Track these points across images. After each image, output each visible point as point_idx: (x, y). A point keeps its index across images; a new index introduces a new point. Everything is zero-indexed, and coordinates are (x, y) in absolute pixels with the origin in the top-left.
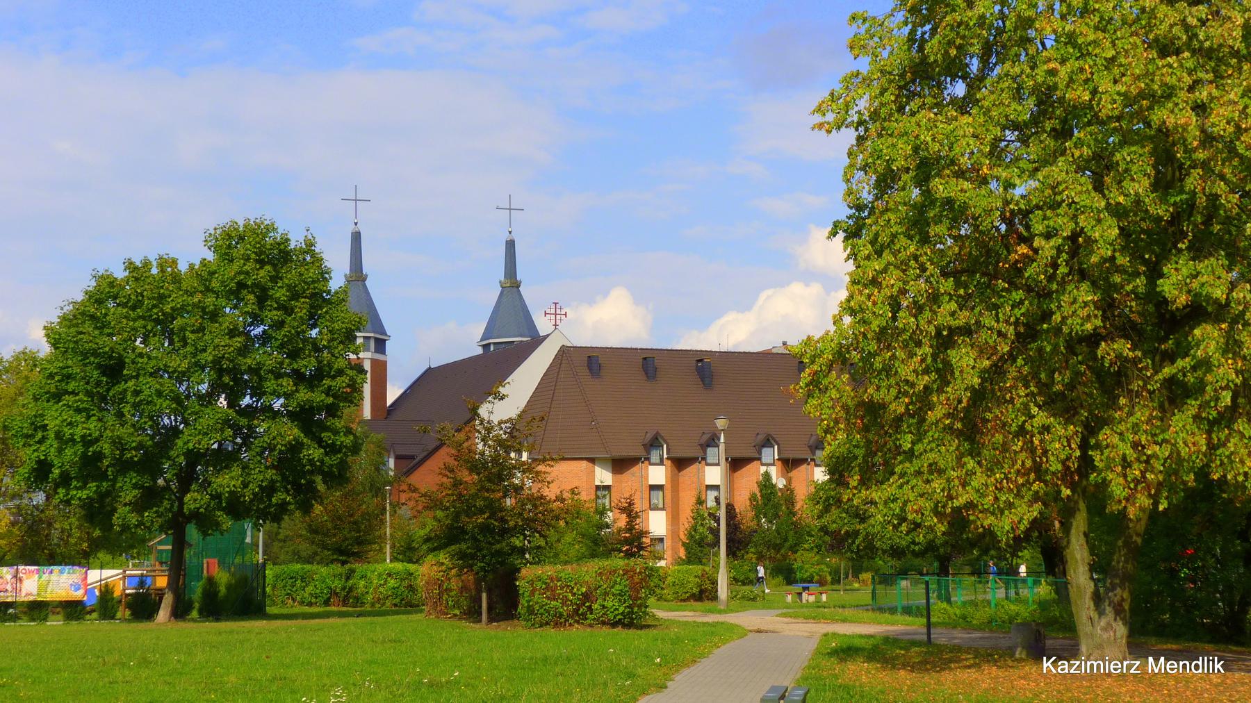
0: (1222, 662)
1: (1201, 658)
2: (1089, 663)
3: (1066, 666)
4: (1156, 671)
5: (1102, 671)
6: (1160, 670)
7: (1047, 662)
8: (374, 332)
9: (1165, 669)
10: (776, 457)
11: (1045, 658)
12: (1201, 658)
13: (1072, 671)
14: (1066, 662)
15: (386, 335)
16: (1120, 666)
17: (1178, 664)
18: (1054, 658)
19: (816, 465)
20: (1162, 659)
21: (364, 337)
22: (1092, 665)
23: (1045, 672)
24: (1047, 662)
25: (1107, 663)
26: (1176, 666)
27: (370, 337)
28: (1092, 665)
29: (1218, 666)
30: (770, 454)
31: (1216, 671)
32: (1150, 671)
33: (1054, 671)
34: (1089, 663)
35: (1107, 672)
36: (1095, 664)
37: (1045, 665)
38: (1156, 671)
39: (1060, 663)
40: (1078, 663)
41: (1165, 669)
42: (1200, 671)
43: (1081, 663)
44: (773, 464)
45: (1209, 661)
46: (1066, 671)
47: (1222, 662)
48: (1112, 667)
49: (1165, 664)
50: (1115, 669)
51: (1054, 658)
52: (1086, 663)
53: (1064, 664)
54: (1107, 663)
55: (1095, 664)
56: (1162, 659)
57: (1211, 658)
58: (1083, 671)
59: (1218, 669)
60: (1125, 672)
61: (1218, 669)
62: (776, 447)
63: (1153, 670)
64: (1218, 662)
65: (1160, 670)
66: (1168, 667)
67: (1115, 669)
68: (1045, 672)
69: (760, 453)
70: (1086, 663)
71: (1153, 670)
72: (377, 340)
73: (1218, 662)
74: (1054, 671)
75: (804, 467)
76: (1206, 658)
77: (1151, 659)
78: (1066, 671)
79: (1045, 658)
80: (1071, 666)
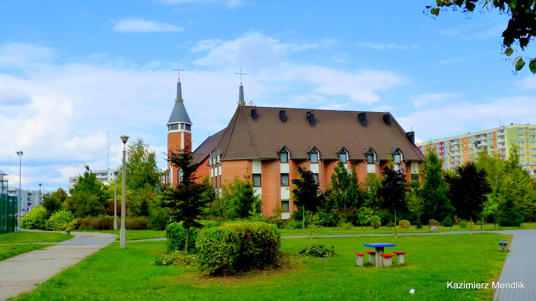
3: (457, 286)
8: (185, 121)
10: (348, 159)
11: (448, 282)
15: (191, 123)
18: (452, 282)
19: (368, 163)
21: (181, 124)
23: (448, 288)
27: (183, 124)
30: (344, 158)
33: (452, 288)
37: (448, 285)
39: (454, 284)
44: (346, 163)
46: (457, 288)
51: (452, 282)
62: (347, 154)
68: (448, 288)
69: (339, 157)
72: (187, 125)
74: (452, 288)
75: (362, 165)
78: (457, 288)
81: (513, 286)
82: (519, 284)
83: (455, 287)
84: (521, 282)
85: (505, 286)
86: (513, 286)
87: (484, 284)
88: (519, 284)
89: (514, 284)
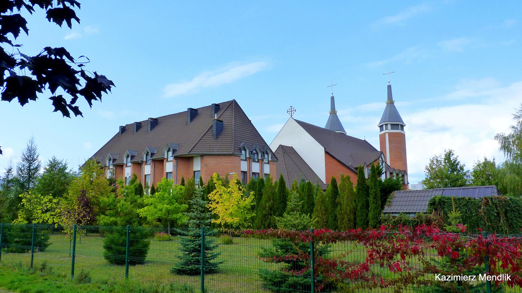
0: (510, 276)
1: (501, 274)
2: (454, 276)
3: (445, 278)
4: (483, 280)
5: (460, 280)
6: (484, 279)
7: (437, 276)
9: (486, 279)
12: (501, 274)
13: (447, 280)
14: (445, 276)
16: (467, 278)
17: (492, 277)
18: (440, 274)
20: (485, 275)
22: (456, 277)
24: (437, 276)
25: (462, 276)
26: (491, 278)
28: (456, 278)
29: (508, 278)
31: (507, 280)
32: (480, 280)
34: (454, 276)
35: (462, 280)
36: (457, 277)
37: (436, 277)
38: (483, 280)
39: (442, 277)
40: (450, 276)
41: (486, 279)
42: (501, 280)
43: (451, 277)
45: (504, 275)
46: (445, 280)
47: (510, 276)
48: (464, 278)
49: (487, 276)
50: (465, 279)
51: (440, 274)
52: (453, 277)
53: (443, 277)
54: (462, 276)
55: (457, 277)
56: (485, 275)
57: (505, 274)
58: (452, 280)
59: (508, 279)
60: (469, 280)
61: (508, 279)
63: (481, 279)
64: (508, 276)
65: (484, 279)
66: (487, 278)
67: (465, 279)
70: (453, 277)
71: (481, 279)
73: (508, 276)
76: (503, 274)
77: (480, 275)
79: (436, 274)
80: (447, 278)
81: (499, 278)
82: (505, 276)
83: (444, 279)
84: (507, 274)
85: (492, 279)
86: (499, 278)
87: (471, 276)
88: (505, 276)
89: (501, 276)
